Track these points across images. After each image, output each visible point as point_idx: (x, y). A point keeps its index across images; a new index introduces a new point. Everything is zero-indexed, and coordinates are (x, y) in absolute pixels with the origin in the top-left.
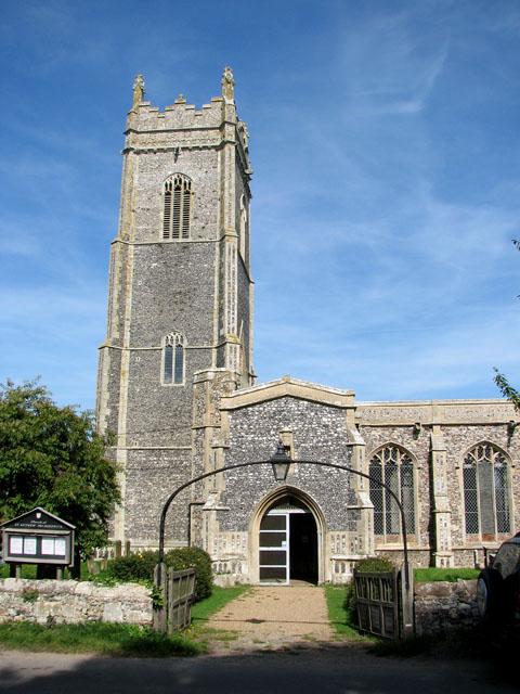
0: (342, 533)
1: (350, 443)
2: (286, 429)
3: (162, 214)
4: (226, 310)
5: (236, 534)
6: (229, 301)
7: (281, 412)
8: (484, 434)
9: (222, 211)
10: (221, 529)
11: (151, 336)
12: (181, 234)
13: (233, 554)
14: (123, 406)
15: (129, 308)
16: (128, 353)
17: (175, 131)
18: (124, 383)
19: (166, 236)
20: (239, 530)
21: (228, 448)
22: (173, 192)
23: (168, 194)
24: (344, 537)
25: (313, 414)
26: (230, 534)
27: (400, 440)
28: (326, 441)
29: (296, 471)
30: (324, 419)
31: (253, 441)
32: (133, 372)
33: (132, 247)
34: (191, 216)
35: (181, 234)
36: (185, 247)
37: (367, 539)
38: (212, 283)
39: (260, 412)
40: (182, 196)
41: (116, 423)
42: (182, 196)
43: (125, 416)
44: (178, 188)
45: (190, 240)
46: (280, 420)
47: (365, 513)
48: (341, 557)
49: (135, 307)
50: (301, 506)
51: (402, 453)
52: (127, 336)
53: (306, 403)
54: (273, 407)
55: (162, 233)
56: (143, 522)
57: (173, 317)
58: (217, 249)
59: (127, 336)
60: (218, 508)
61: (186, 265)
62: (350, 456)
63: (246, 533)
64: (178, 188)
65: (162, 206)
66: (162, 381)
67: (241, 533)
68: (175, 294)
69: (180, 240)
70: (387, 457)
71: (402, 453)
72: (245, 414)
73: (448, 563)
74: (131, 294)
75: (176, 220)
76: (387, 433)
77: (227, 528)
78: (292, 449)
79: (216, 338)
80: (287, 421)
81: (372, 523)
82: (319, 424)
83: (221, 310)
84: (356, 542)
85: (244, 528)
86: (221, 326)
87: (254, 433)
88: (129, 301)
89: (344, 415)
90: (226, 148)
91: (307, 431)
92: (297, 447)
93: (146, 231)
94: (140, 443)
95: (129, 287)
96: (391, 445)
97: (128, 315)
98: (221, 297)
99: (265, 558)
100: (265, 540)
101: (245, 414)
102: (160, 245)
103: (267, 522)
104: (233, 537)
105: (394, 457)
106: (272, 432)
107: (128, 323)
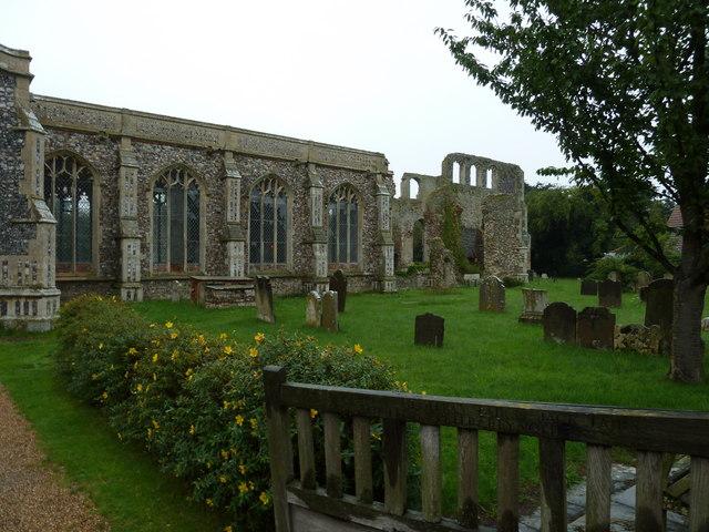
1: (20, 127)
8: (180, 156)
27: (78, 150)
37: (46, 267)
47: (42, 231)
51: (79, 165)
62: (20, 146)
70: (59, 167)
71: (79, 165)
73: (135, 295)
76: (61, 137)
81: (54, 244)
84: (27, 271)
89: (13, 85)
96: (66, 153)
105: (69, 168)
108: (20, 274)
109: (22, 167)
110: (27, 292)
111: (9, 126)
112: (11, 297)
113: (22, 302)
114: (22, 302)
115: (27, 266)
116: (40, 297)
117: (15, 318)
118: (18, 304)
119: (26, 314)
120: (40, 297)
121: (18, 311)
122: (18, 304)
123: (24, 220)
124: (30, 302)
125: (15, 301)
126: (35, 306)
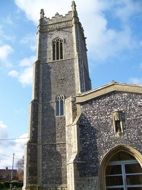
3: (52, 52)
5: (90, 178)
7: (112, 101)
14: (40, 127)
19: (54, 59)
21: (82, 125)
25: (131, 100)
41: (37, 134)
43: (41, 131)
45: (63, 59)
52: (41, 99)
53: (126, 94)
54: (107, 99)
56: (50, 176)
59: (41, 99)
60: (77, 162)
63: (97, 178)
64: (58, 43)
66: (55, 115)
67: (93, 178)
74: (41, 83)
75: (58, 51)
77: (85, 175)
82: (136, 105)
87: (97, 115)
88: (41, 85)
94: (47, 142)
95: (41, 80)
97: (41, 90)
101: (91, 104)
107: (40, 93)
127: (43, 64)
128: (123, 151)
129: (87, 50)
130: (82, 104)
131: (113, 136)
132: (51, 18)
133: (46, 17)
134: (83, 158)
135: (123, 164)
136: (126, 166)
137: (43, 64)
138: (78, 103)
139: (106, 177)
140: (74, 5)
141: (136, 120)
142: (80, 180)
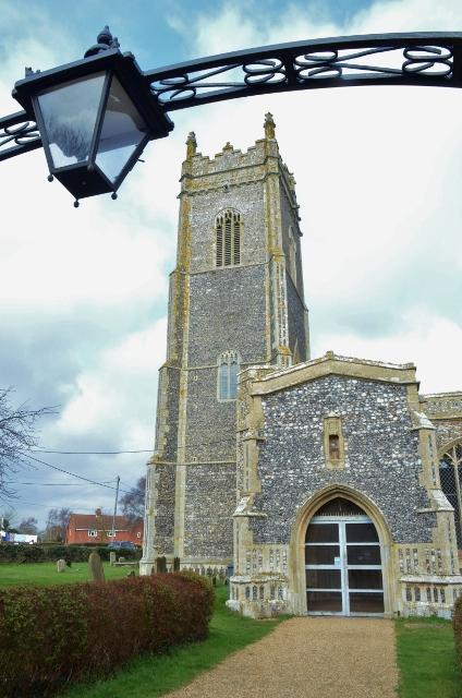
0: (413, 546)
1: (415, 427)
2: (332, 414)
4: (277, 324)
5: (274, 547)
6: (279, 316)
7: (324, 394)
9: (270, 236)
10: (255, 541)
11: (208, 355)
12: (232, 261)
13: (271, 574)
14: (182, 424)
15: (187, 332)
16: (186, 373)
17: (224, 172)
18: (183, 402)
19: (219, 264)
20: (279, 542)
21: (262, 441)
22: (224, 226)
23: (219, 227)
24: (415, 551)
25: (364, 394)
26: (267, 547)
28: (383, 427)
29: (347, 465)
30: (379, 400)
31: (292, 431)
32: (191, 392)
33: (188, 277)
34: (241, 244)
35: (232, 261)
36: (238, 271)
37: (449, 554)
38: (263, 302)
39: (299, 396)
40: (232, 228)
42: (232, 228)
44: (228, 221)
46: (324, 404)
47: (441, 518)
48: (413, 579)
49: (194, 328)
50: (358, 511)
52: (186, 358)
53: (355, 382)
54: (315, 389)
55: (215, 262)
56: (201, 538)
57: (227, 337)
58: (267, 270)
59: (186, 358)
60: (250, 514)
61: (238, 287)
62: (416, 443)
63: (287, 547)
64: (228, 221)
65: (215, 238)
66: (218, 397)
67: (281, 546)
68: (229, 314)
69: (232, 266)
72: (282, 400)
75: (228, 244)
77: (264, 540)
78: (341, 439)
79: (269, 352)
80: (332, 405)
82: (373, 406)
83: (272, 326)
84: (433, 558)
85: (283, 540)
86: (273, 340)
87: (293, 421)
89: (405, 393)
90: (270, 179)
91: (359, 415)
92: (347, 435)
93: (201, 262)
94: (199, 458)
95: (187, 313)
97: (186, 339)
98: (272, 314)
99: (314, 579)
100: (312, 555)
101: (282, 400)
102: (214, 273)
103: (313, 532)
104: (271, 552)
106: (315, 419)
107: (186, 346)
108: (428, 561)
109: (419, 462)
110: (435, 579)
111: (406, 428)
112: (423, 583)
113: (432, 588)
114: (432, 588)
115: (433, 554)
116: (446, 584)
117: (427, 604)
118: (428, 590)
119: (436, 601)
120: (446, 584)
121: (429, 598)
122: (428, 590)
123: (426, 510)
124: (439, 588)
125: (425, 587)
126: (442, 593)
127: (192, 275)
128: (342, 496)
129: (301, 234)
130: (264, 397)
131: (323, 466)
132: (212, 158)
133: (200, 155)
134: (261, 506)
135: (342, 521)
136: (348, 527)
137: (192, 275)
138: (258, 395)
139: (307, 548)
140: (270, 125)
141: (372, 435)
142: (254, 550)
